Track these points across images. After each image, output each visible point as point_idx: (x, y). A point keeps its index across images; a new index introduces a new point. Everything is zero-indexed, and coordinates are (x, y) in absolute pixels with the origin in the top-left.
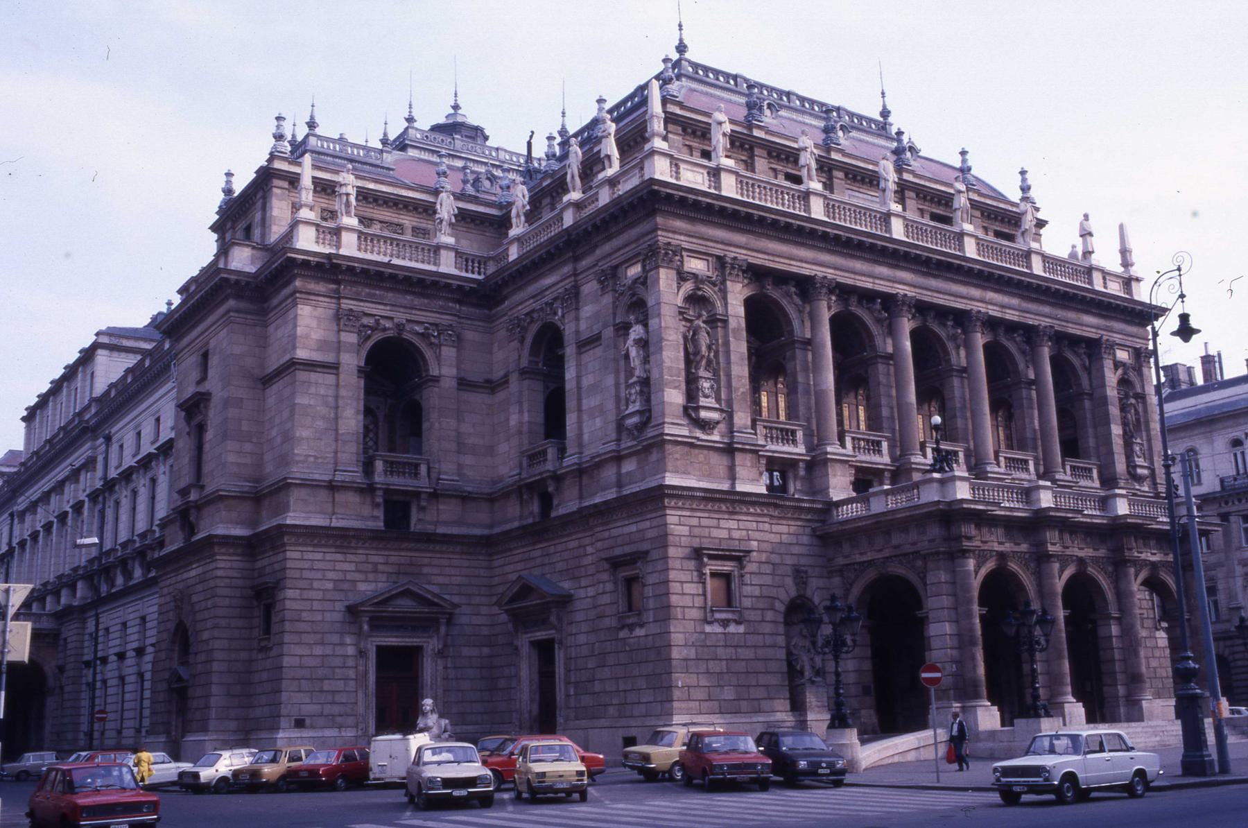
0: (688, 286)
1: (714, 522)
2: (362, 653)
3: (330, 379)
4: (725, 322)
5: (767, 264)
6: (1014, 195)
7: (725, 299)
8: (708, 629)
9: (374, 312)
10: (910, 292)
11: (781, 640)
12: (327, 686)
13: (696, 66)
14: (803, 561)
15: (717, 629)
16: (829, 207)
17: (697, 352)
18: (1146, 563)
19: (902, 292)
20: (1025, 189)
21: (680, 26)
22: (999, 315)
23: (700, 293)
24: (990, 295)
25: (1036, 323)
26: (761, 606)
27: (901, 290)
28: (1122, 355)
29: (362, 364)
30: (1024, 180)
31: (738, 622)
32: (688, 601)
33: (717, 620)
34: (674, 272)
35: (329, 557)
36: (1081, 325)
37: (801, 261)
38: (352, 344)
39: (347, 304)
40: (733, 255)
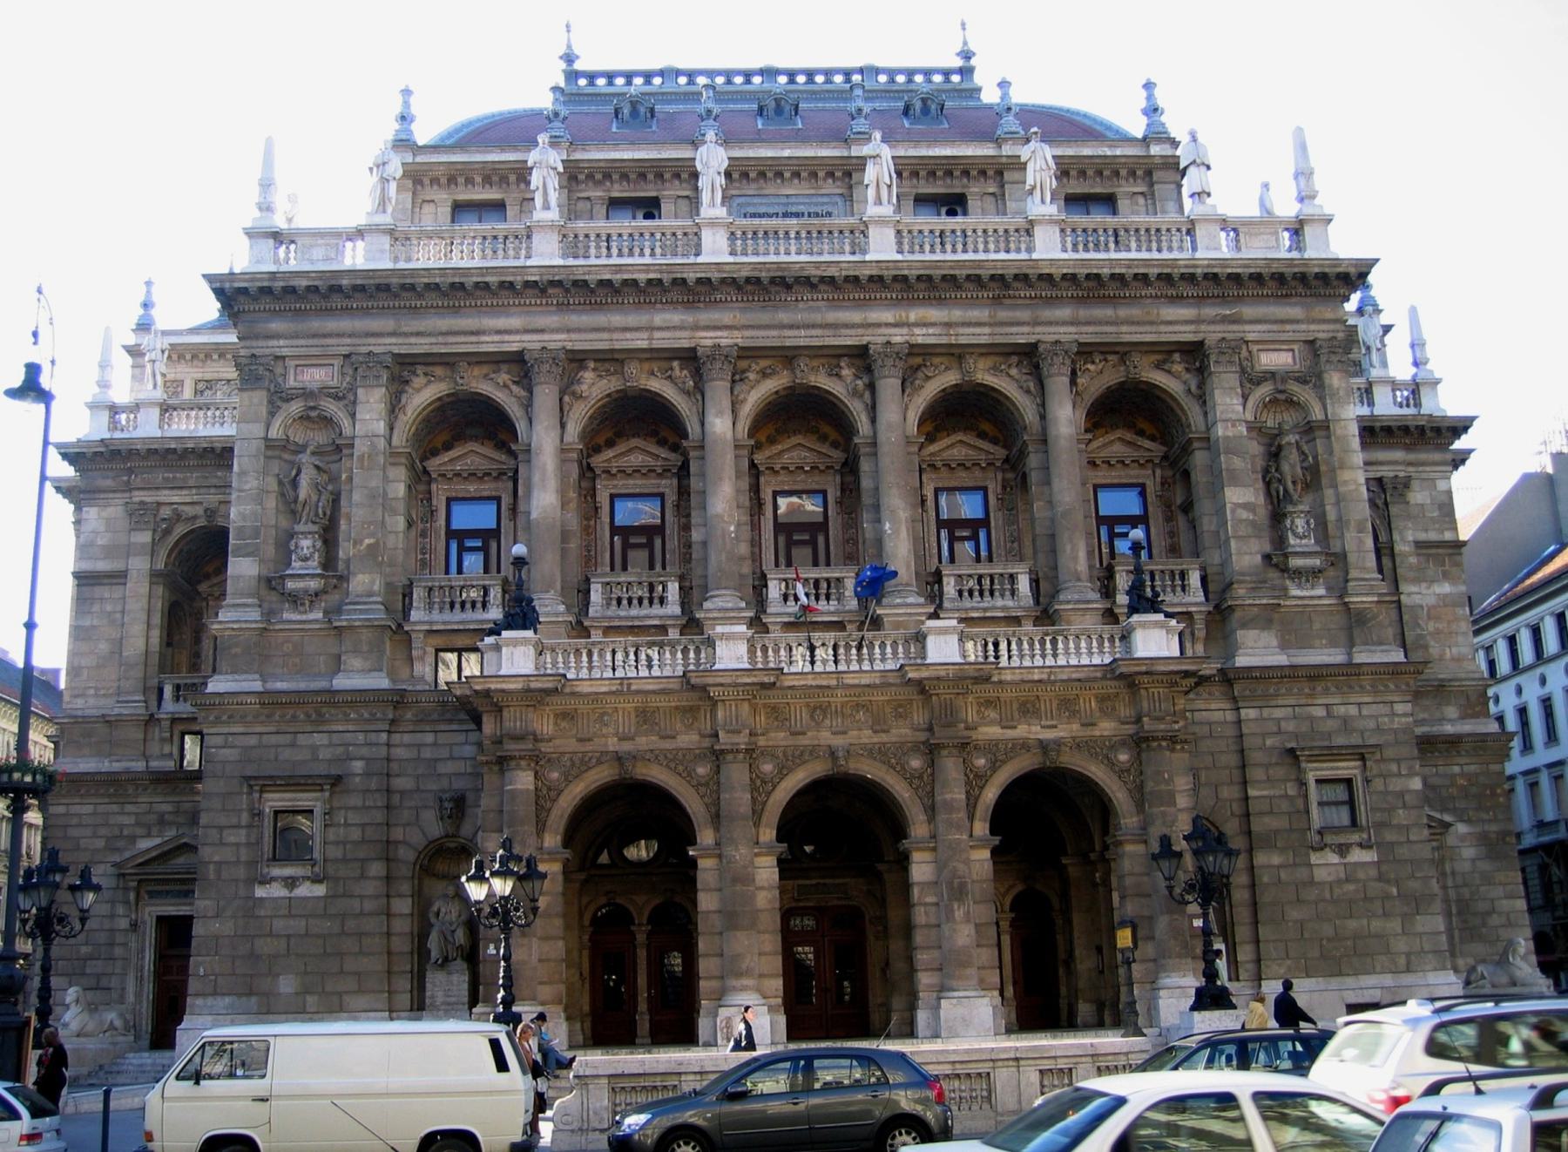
0: (296, 407)
1: (288, 738)
2: (134, 926)
3: (117, 592)
4: (352, 446)
5: (435, 350)
6: (1136, 126)
7: (353, 415)
8: (260, 892)
9: (176, 499)
10: (726, 339)
11: (403, 906)
12: (93, 967)
13: (592, 77)
14: (459, 784)
15: (277, 891)
16: (573, 244)
17: (296, 501)
18: (1024, 745)
19: (709, 342)
20: (1152, 110)
21: (568, 26)
22: (944, 340)
23: (313, 414)
24: (913, 315)
25: (1032, 339)
26: (361, 855)
27: (706, 339)
28: (1271, 360)
29: (160, 566)
30: (1150, 97)
31: (316, 880)
32: (226, 854)
33: (273, 879)
34: (264, 393)
35: (101, 809)
36: (1152, 323)
37: (499, 332)
38: (143, 545)
39: (139, 496)
40: (364, 350)
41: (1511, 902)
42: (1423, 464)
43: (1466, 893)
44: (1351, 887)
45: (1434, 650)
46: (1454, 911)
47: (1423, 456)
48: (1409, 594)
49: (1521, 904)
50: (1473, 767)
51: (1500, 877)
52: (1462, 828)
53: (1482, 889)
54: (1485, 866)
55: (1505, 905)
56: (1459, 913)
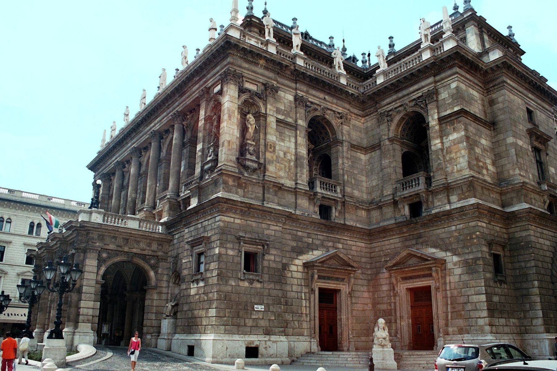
41: (477, 297)
42: (443, 79)
43: (455, 293)
44: (197, 297)
45: (449, 169)
46: (449, 303)
47: (443, 75)
48: (435, 145)
49: (483, 298)
50: (461, 225)
51: (473, 283)
52: (455, 259)
53: (463, 290)
54: (465, 278)
55: (475, 298)
56: (451, 304)
